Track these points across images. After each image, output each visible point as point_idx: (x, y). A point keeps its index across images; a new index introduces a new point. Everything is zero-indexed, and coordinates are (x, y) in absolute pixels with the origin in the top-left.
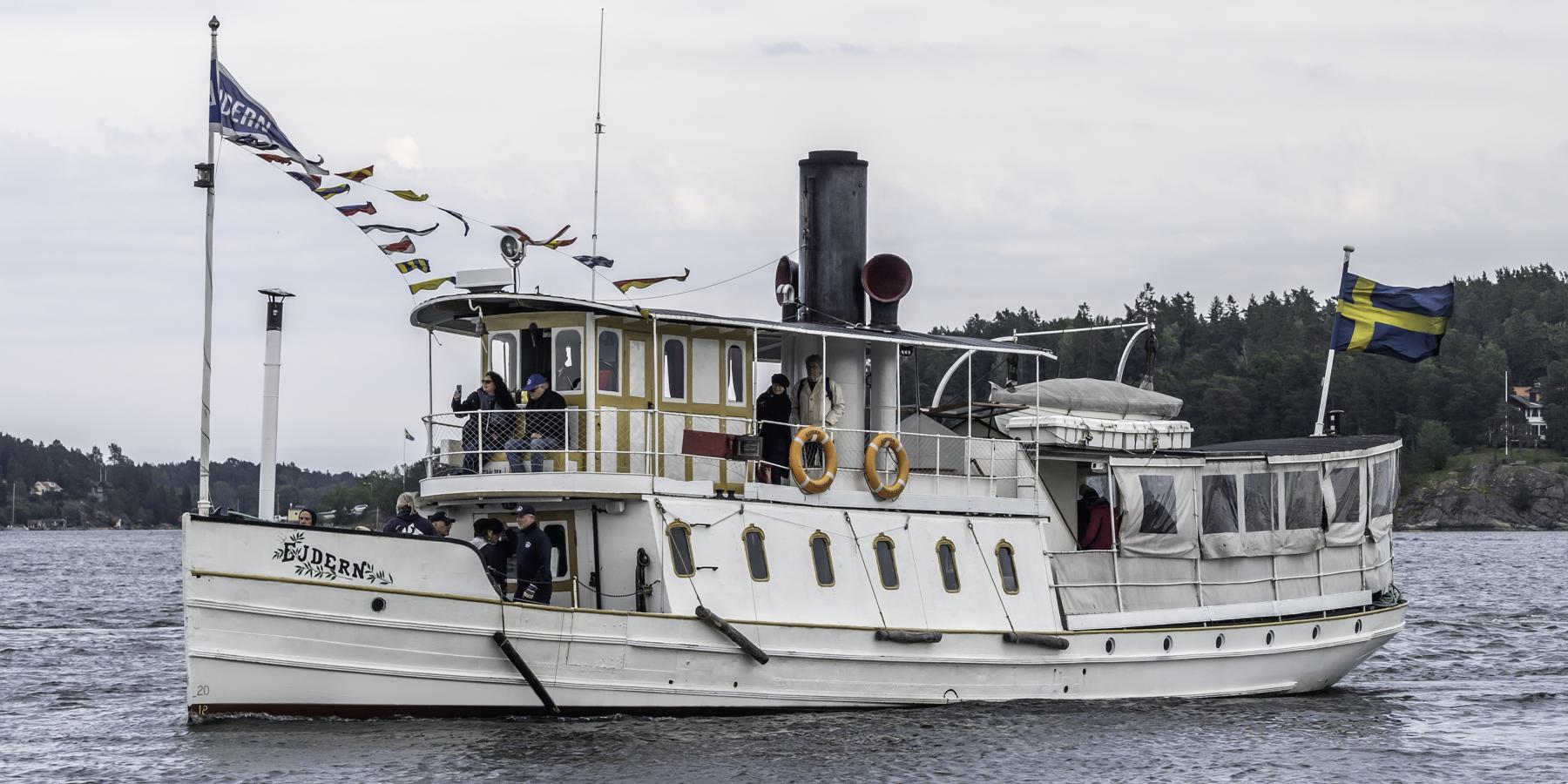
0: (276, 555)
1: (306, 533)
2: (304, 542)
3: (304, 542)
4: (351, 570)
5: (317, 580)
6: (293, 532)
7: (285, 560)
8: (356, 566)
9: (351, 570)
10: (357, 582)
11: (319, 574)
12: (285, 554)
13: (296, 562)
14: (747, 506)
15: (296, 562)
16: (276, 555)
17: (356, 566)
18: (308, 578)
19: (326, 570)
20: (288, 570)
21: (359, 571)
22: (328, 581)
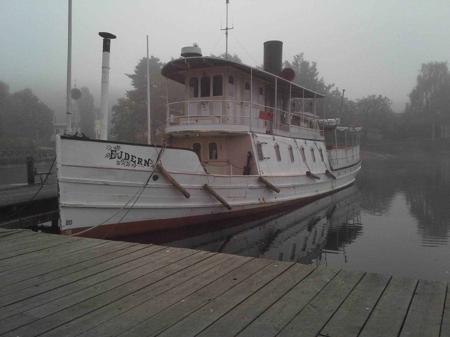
0: (107, 156)
1: (122, 146)
2: (121, 150)
3: (121, 150)
4: (143, 162)
5: (127, 168)
6: (116, 145)
7: (111, 158)
8: (145, 161)
9: (143, 162)
10: (146, 168)
11: (128, 165)
12: (111, 156)
13: (117, 159)
14: (275, 137)
15: (117, 159)
16: (107, 156)
17: (145, 161)
18: (122, 167)
19: (133, 163)
20: (113, 163)
21: (147, 163)
22: (133, 168)
